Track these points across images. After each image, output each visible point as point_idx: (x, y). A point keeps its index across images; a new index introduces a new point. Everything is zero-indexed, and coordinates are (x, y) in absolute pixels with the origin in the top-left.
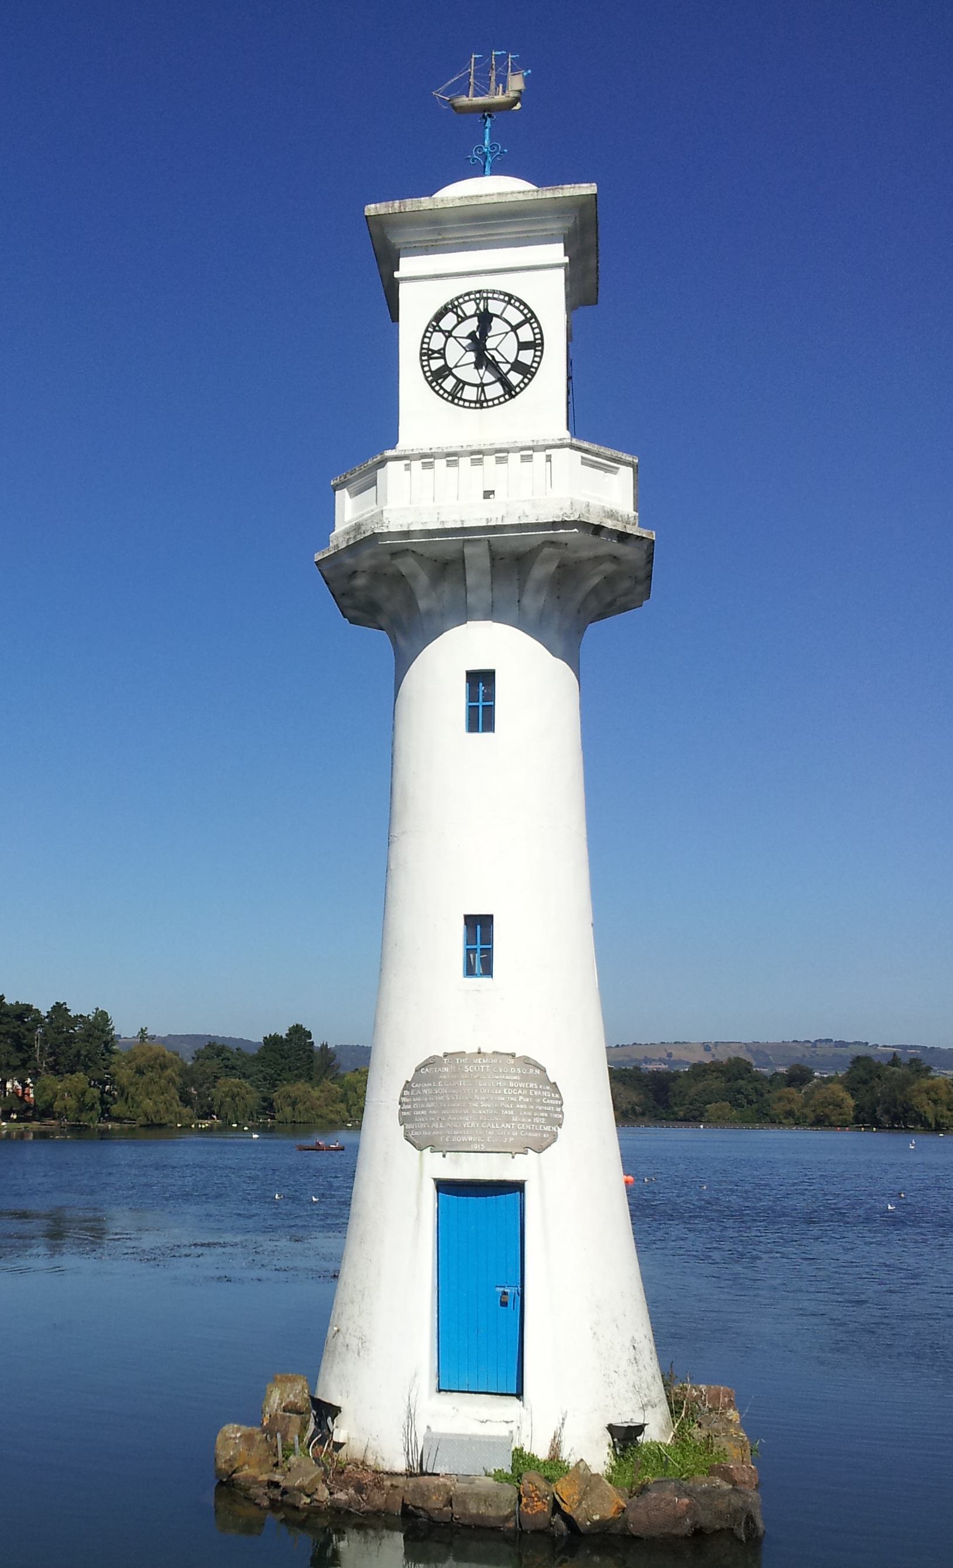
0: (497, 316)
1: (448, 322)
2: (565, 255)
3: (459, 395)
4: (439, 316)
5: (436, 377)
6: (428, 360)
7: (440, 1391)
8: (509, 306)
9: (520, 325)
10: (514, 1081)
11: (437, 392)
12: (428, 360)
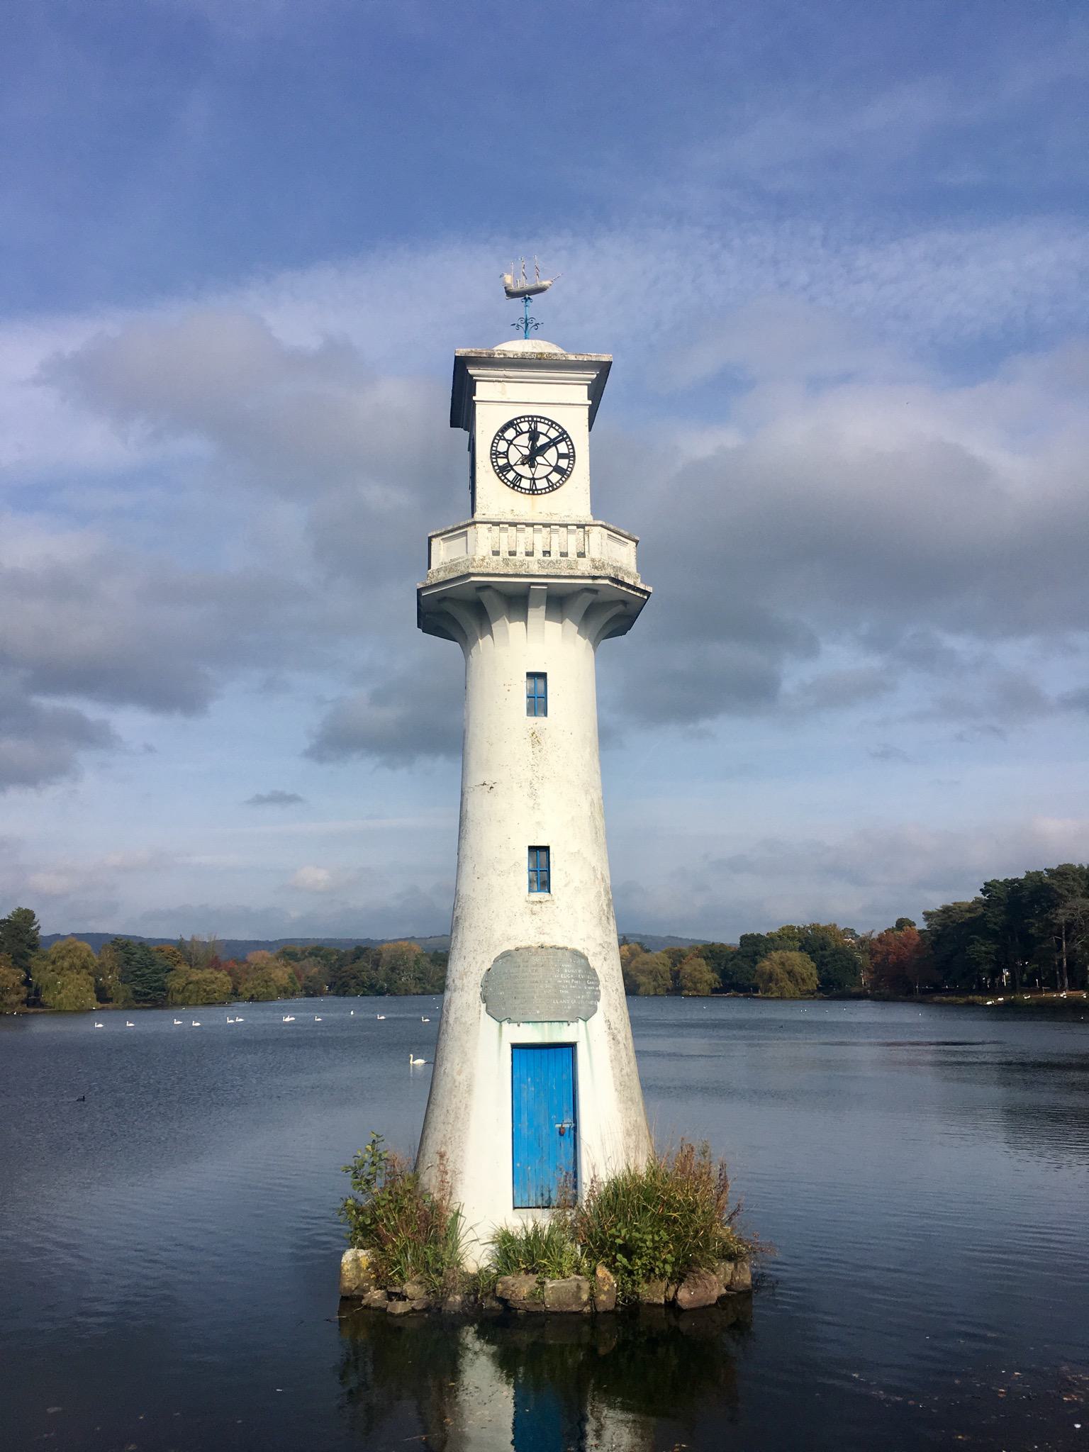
0: (543, 434)
1: (510, 434)
2: (589, 399)
3: (518, 484)
5: (502, 471)
6: (496, 458)
7: (515, 1208)
8: (552, 429)
10: (567, 968)
11: (503, 481)
12: (496, 458)
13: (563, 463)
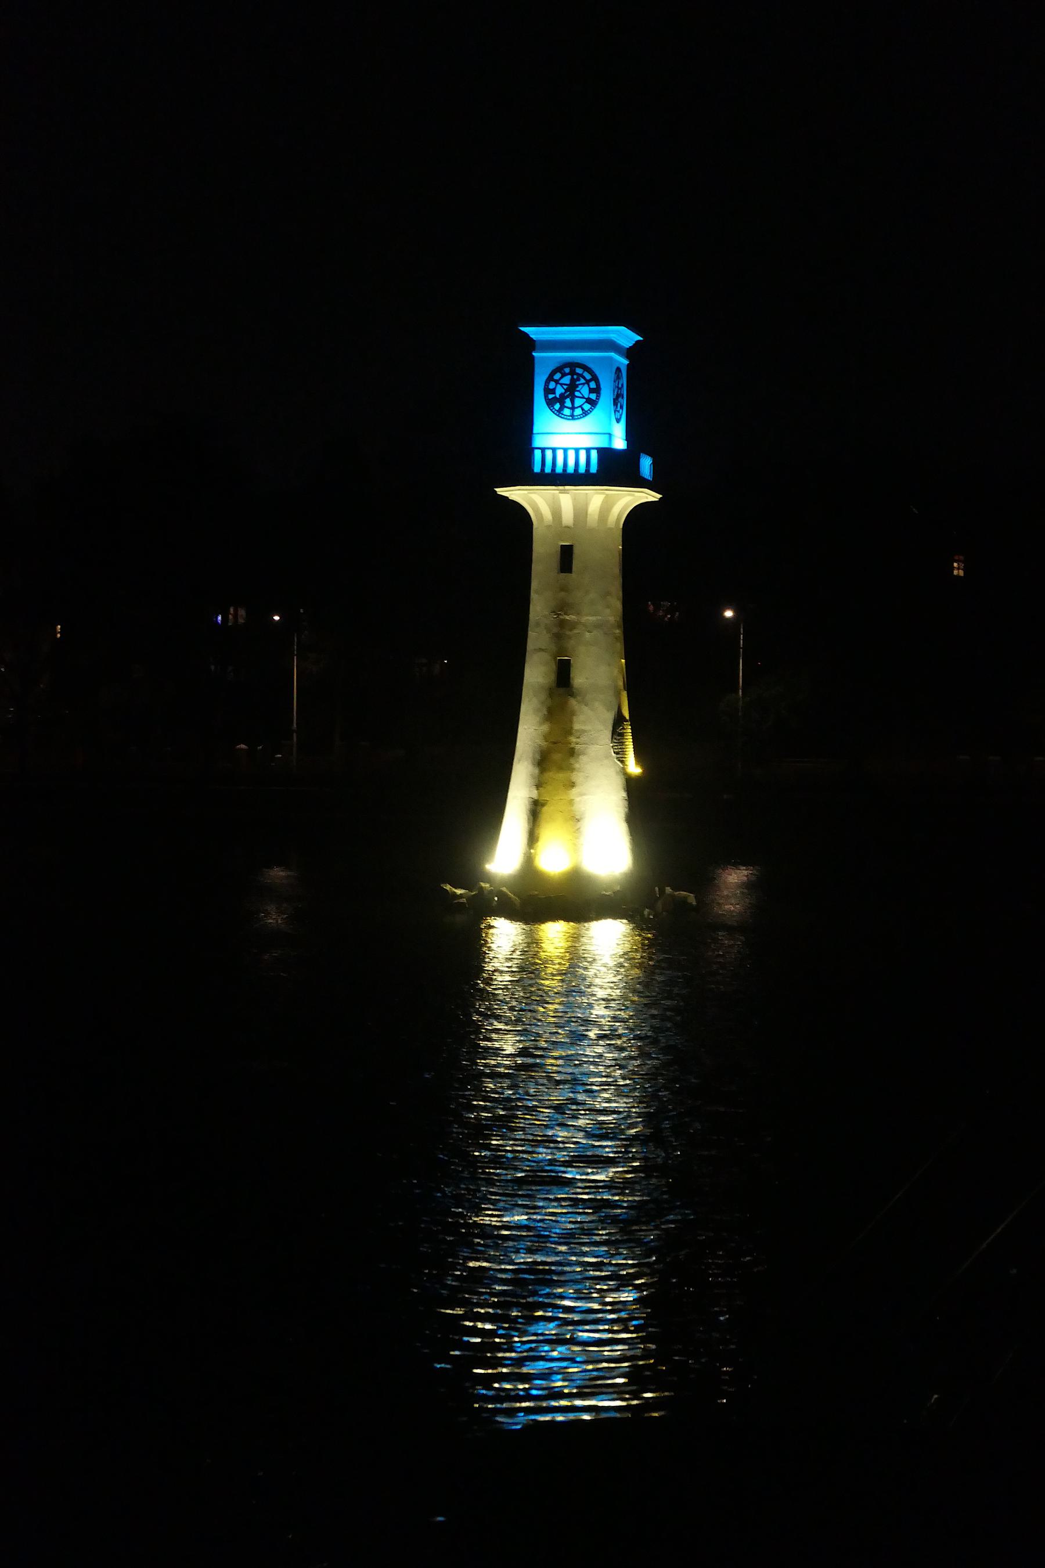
1: (557, 376)
4: (553, 373)
9: (591, 380)
13: (593, 396)
